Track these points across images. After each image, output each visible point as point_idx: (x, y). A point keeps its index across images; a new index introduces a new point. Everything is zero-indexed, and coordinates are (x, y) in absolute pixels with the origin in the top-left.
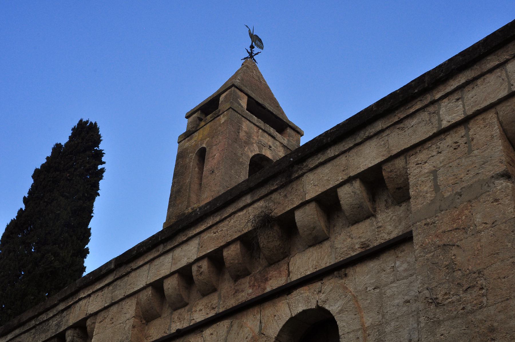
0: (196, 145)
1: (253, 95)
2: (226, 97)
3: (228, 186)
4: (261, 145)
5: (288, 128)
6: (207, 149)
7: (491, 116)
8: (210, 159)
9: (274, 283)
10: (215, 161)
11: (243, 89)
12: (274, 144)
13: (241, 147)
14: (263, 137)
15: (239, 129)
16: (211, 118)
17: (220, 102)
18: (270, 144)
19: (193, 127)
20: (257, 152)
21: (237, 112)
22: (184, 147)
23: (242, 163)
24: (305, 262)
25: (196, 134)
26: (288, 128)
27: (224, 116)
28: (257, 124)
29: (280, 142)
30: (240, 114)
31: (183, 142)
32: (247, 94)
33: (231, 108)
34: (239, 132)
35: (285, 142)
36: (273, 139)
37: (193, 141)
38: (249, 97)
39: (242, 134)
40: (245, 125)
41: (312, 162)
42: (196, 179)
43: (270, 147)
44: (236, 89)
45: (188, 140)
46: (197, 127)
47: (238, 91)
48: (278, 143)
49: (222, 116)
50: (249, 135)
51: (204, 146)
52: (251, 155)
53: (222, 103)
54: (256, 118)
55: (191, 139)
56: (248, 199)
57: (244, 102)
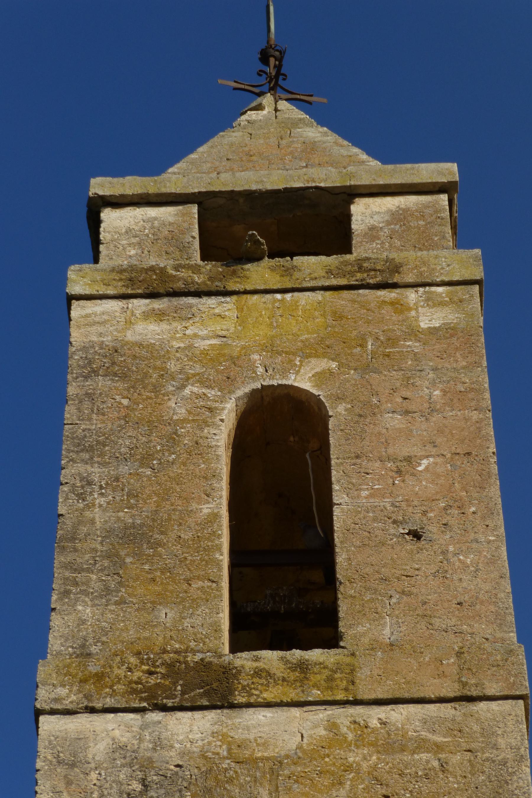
2: (399, 217)
6: (338, 413)
22: (130, 336)
27: (432, 302)
45: (160, 316)
51: (303, 380)
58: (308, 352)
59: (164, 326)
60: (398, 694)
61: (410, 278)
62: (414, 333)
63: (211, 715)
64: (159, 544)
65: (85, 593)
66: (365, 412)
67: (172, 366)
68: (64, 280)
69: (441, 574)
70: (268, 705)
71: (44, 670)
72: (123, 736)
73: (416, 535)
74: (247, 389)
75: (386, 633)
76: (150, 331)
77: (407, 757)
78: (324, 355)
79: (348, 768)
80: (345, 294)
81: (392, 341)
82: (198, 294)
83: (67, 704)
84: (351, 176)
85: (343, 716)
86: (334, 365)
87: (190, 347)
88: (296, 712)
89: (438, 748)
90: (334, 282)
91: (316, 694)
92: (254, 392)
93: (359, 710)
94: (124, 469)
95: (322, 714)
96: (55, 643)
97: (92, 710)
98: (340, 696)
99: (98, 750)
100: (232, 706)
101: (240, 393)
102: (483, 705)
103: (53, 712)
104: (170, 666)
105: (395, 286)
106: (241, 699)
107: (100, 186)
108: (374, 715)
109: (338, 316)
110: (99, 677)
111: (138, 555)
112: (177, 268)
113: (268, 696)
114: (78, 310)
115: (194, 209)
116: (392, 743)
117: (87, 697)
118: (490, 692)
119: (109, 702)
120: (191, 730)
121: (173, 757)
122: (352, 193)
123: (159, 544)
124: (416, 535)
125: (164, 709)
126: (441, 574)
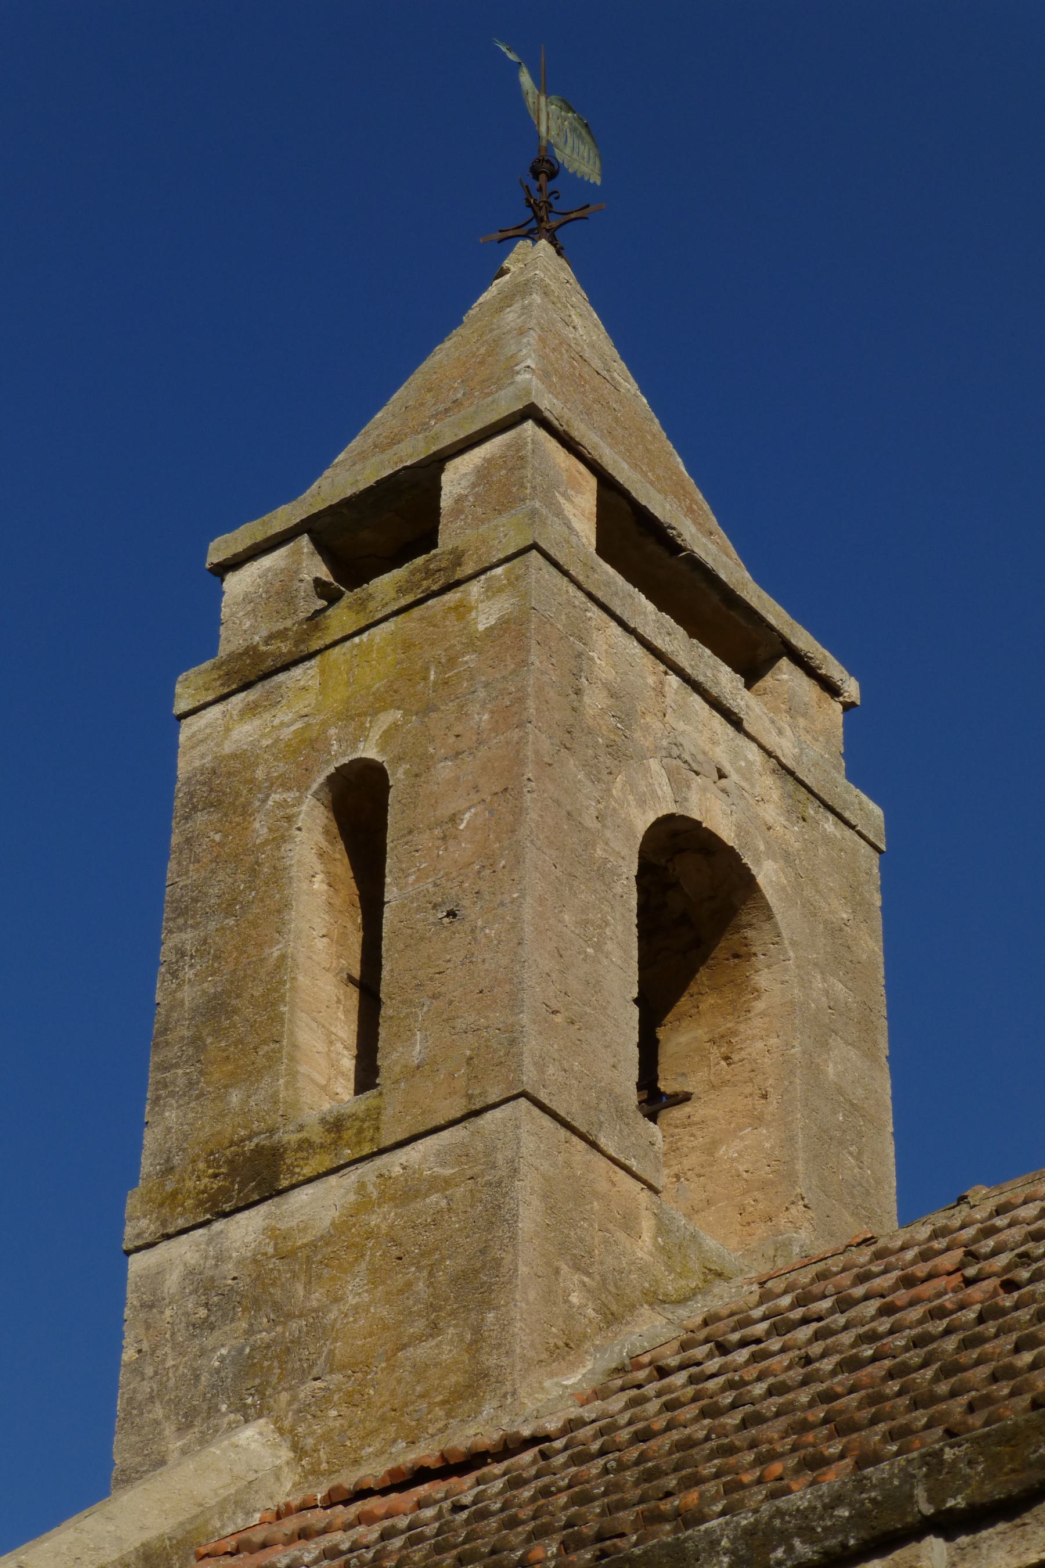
0: (309, 744)
1: (624, 473)
2: (483, 474)
3: (555, 1004)
4: (685, 767)
5: (784, 662)
6: (397, 777)
8: (424, 839)
10: (463, 850)
11: (575, 434)
12: (736, 754)
14: (688, 721)
16: (401, 591)
17: (446, 502)
18: (721, 755)
19: (281, 635)
21: (565, 573)
22: (228, 748)
26: (784, 662)
27: (492, 592)
28: (658, 643)
29: (761, 746)
30: (580, 587)
31: (215, 711)
32: (595, 467)
33: (535, 546)
34: (578, 692)
36: (730, 730)
37: (283, 715)
38: (609, 489)
39: (595, 701)
42: (321, 944)
43: (722, 775)
44: (542, 434)
45: (251, 710)
46: (303, 637)
47: (552, 445)
48: (753, 753)
49: (475, 588)
52: (643, 821)
53: (457, 511)
54: (650, 607)
55: (272, 703)
57: (580, 512)
58: (379, 704)
59: (257, 722)
60: (415, 1131)
61: (468, 569)
62: (472, 643)
63: (263, 1208)
64: (235, 1011)
65: (172, 1094)
66: (424, 765)
67: (260, 773)
68: (170, 697)
69: (469, 959)
70: (309, 1180)
71: (133, 1203)
72: (192, 1258)
73: (452, 914)
74: (321, 779)
75: (416, 1052)
76: (245, 733)
77: (418, 1205)
78: (384, 709)
79: (370, 1235)
80: (416, 612)
81: (452, 661)
82: (286, 667)
83: (148, 1238)
84: (436, 438)
85: (367, 1171)
86: (399, 714)
87: (277, 741)
88: (333, 1179)
89: (448, 1182)
90: (404, 602)
91: (348, 1154)
92: (330, 779)
93: (385, 1158)
94: (212, 925)
95: (352, 1176)
96: (147, 1165)
97: (168, 1237)
98: (366, 1150)
99: (172, 1281)
100: (280, 1193)
101: (315, 786)
102: (489, 1116)
103: (138, 1249)
104: (230, 1162)
105: (458, 583)
106: (285, 1183)
107: (219, 550)
108: (395, 1163)
109: (407, 646)
110: (174, 1194)
111: (216, 1032)
112: (269, 639)
113: (308, 1171)
114: (187, 730)
115: (305, 540)
116: (406, 1192)
117: (164, 1224)
118: (492, 1099)
119: (181, 1223)
120: (245, 1230)
121: (229, 1268)
122: (438, 461)
123: (235, 1011)
124: (452, 914)
125: (226, 1215)
126: (469, 959)
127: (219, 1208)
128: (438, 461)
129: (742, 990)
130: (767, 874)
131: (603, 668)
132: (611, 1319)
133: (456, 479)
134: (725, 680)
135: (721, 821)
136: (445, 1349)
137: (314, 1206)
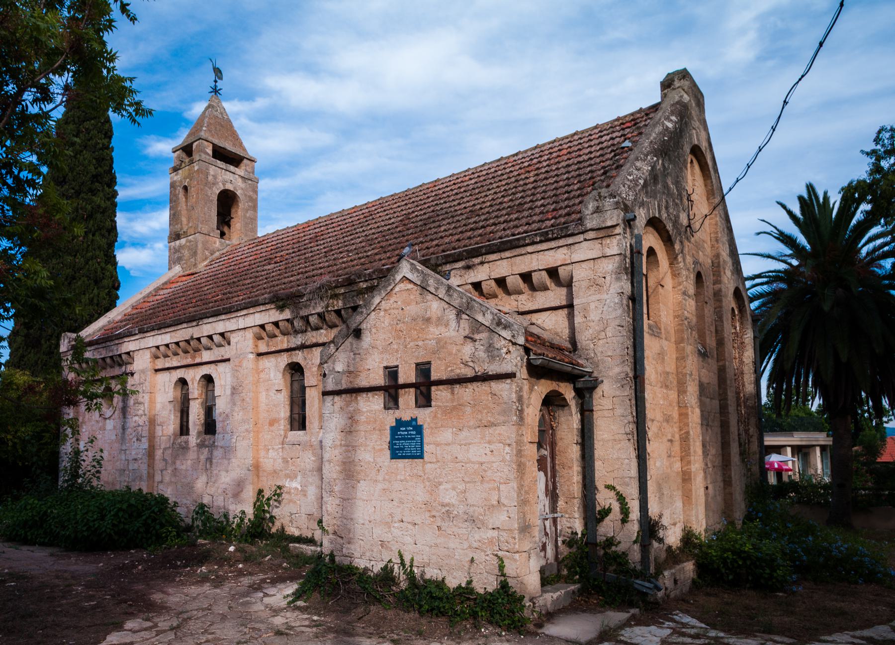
0: (181, 181)
1: (216, 142)
7: (250, 330)
9: (198, 360)
13: (210, 188)
15: (207, 174)
20: (222, 188)
23: (212, 201)
24: (206, 356)
25: (180, 171)
35: (242, 174)
39: (210, 178)
40: (212, 170)
41: (206, 321)
50: (215, 177)
52: (218, 192)
56: (185, 325)
120: (178, 242)
122: (192, 143)
127: (175, 240)
128: (192, 143)
129: (238, 206)
130: (239, 193)
131: (212, 172)
132: (212, 254)
133: (195, 145)
134: (232, 168)
135: (230, 187)
136: (193, 260)
137: (183, 241)
